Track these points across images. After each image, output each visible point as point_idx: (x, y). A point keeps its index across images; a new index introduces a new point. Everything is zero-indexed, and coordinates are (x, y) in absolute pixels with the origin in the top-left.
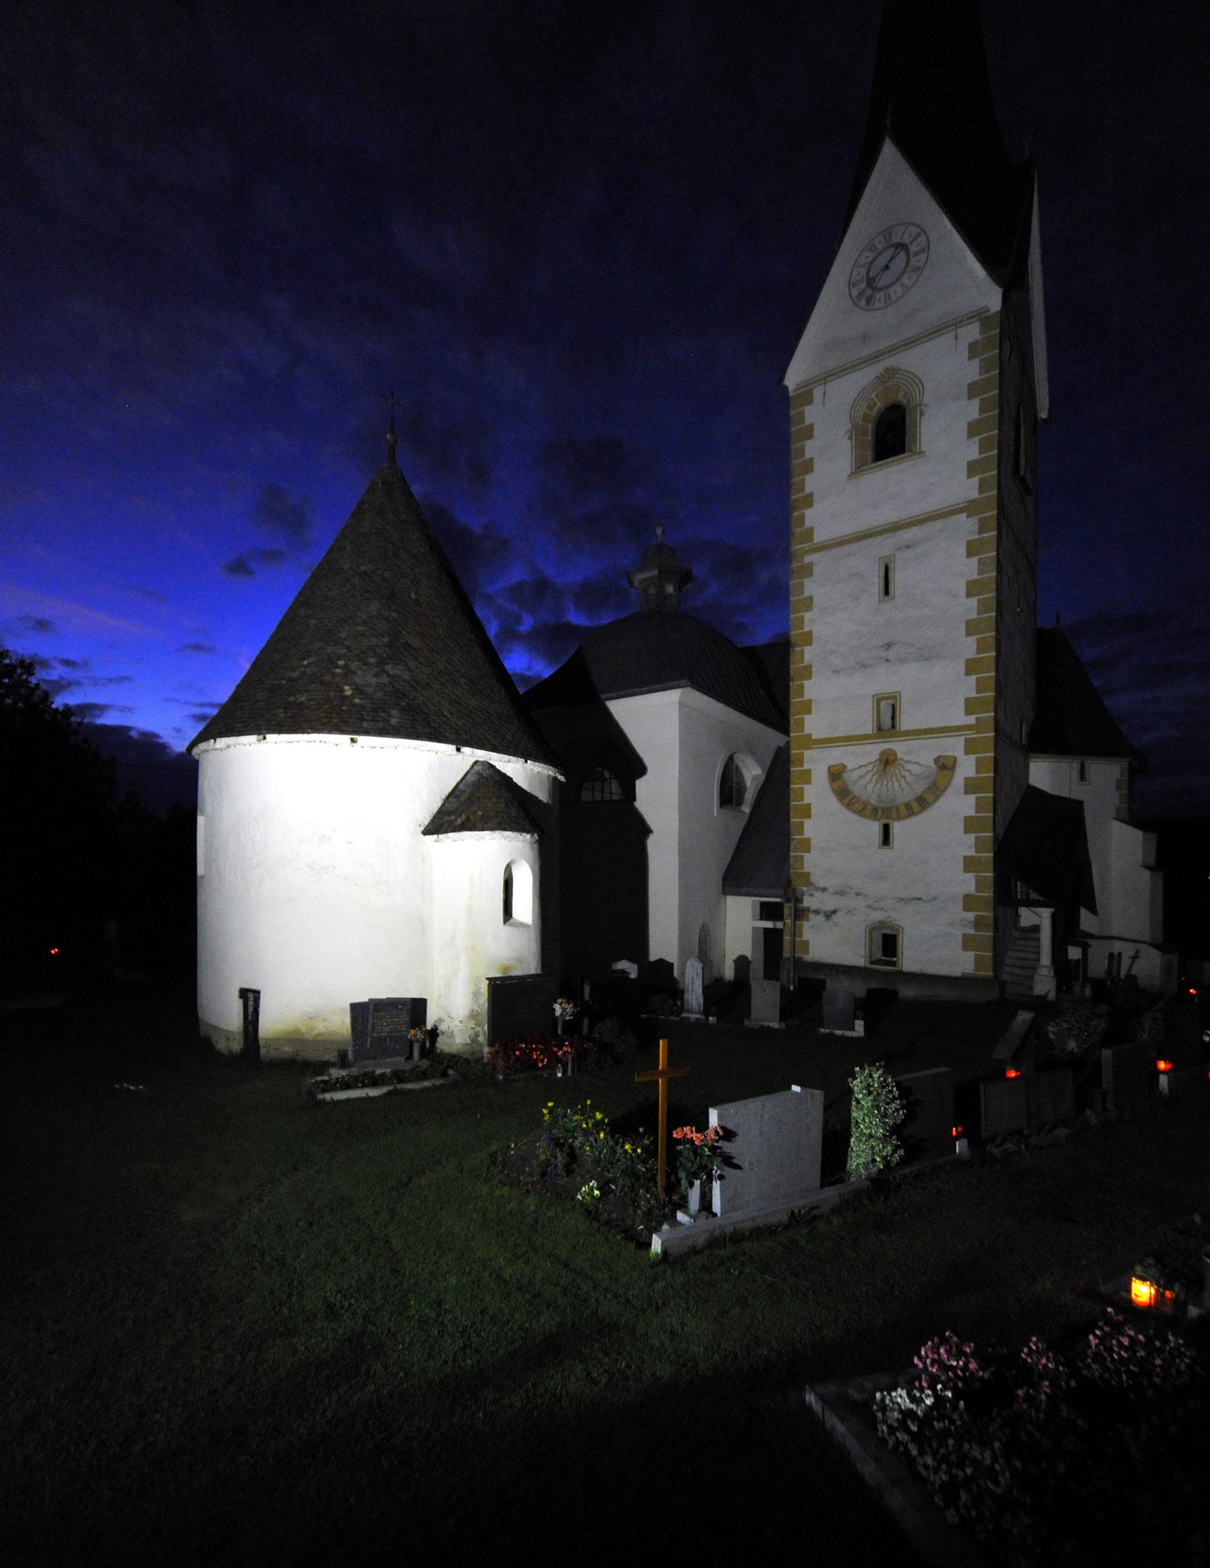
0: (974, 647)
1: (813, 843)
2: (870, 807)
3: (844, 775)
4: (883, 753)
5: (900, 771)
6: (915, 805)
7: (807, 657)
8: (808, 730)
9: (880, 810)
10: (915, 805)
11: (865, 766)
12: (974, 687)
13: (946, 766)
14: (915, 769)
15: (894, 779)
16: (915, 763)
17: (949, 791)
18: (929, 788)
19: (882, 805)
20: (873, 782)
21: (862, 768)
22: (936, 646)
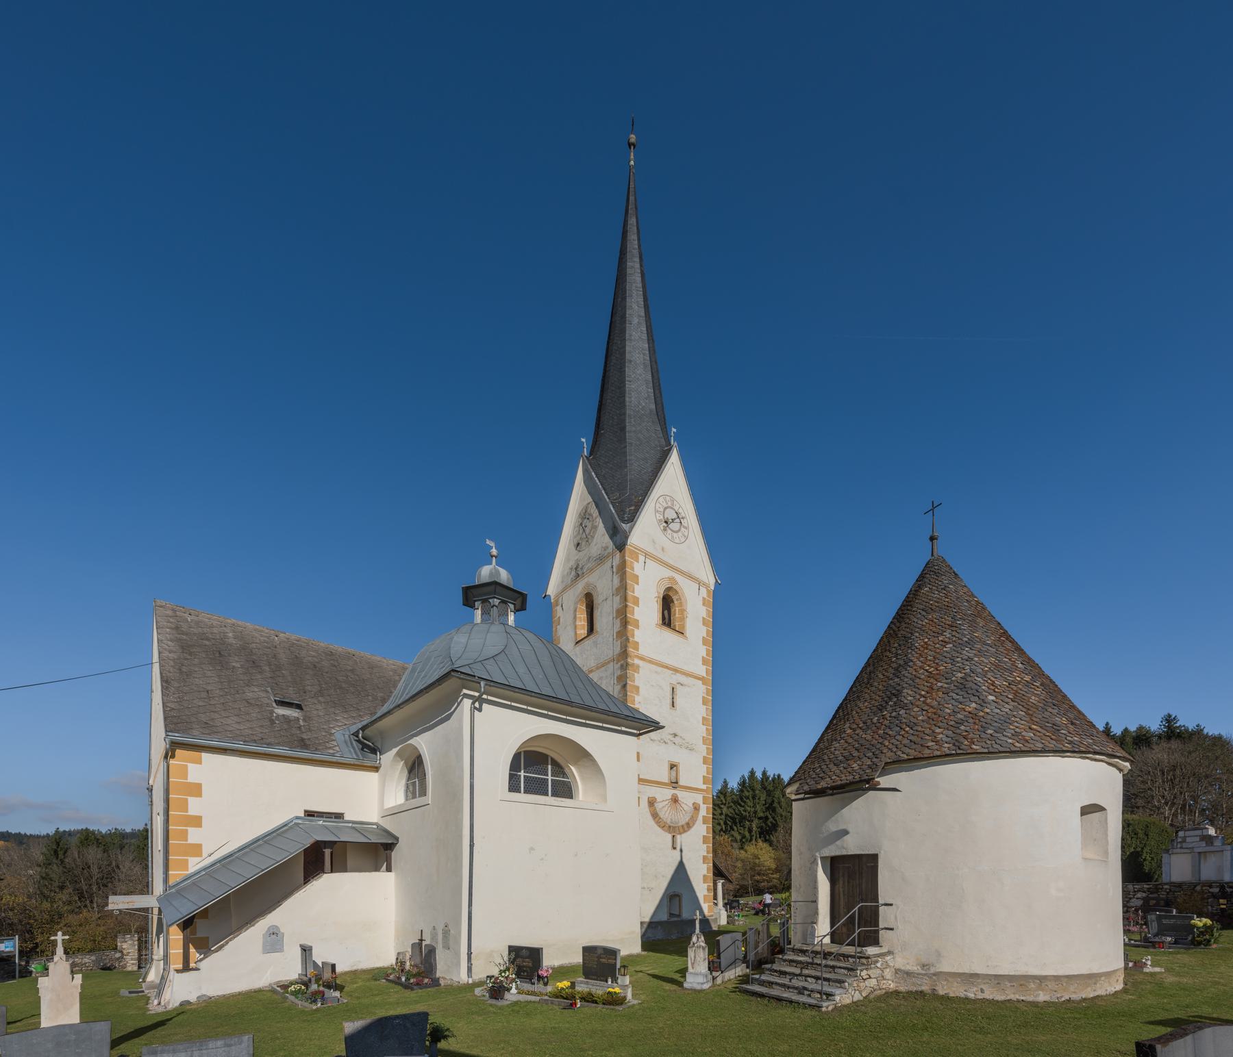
3: (656, 805)
4: (672, 796)
10: (685, 827)
13: (696, 808)
14: (686, 808)
17: (697, 822)
19: (672, 825)
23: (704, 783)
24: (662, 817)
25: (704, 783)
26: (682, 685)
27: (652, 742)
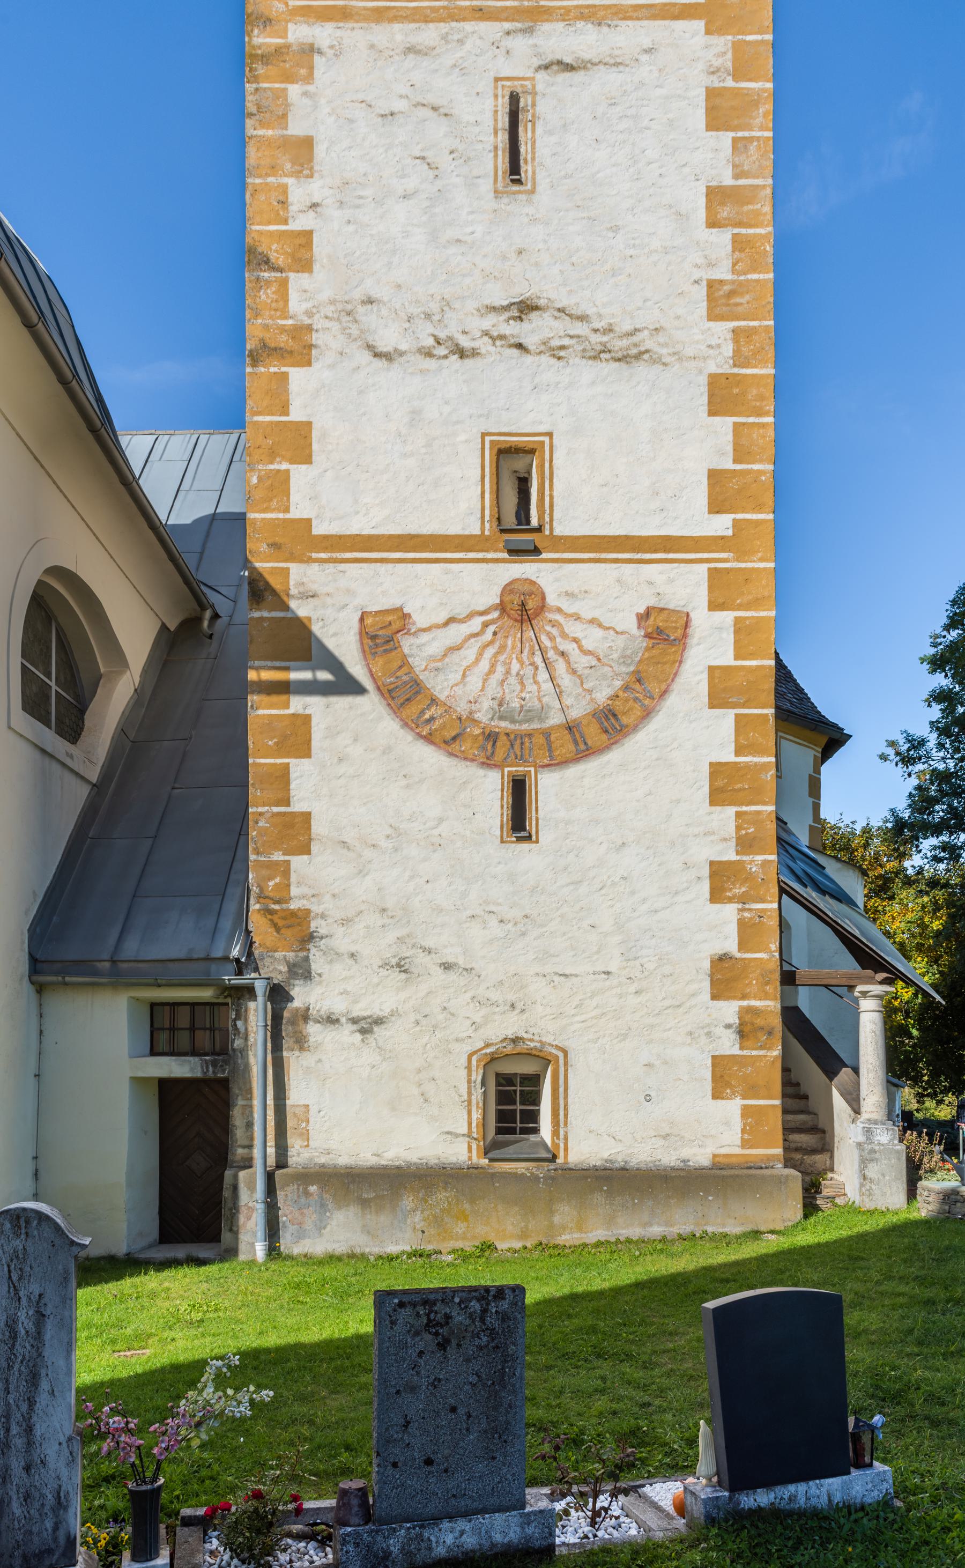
0: (728, 349)
1: (318, 828)
2: (477, 731)
3: (407, 644)
4: (508, 589)
5: (552, 638)
6: (593, 733)
7: (296, 305)
8: (299, 508)
9: (503, 738)
10: (593, 733)
11: (462, 621)
12: (730, 448)
14: (593, 638)
15: (538, 659)
16: (592, 621)
18: (626, 688)
20: (484, 665)
21: (453, 627)
22: (637, 330)
23: (716, 506)
24: (442, 697)
25: (716, 506)
26: (570, 68)
27: (382, 363)
